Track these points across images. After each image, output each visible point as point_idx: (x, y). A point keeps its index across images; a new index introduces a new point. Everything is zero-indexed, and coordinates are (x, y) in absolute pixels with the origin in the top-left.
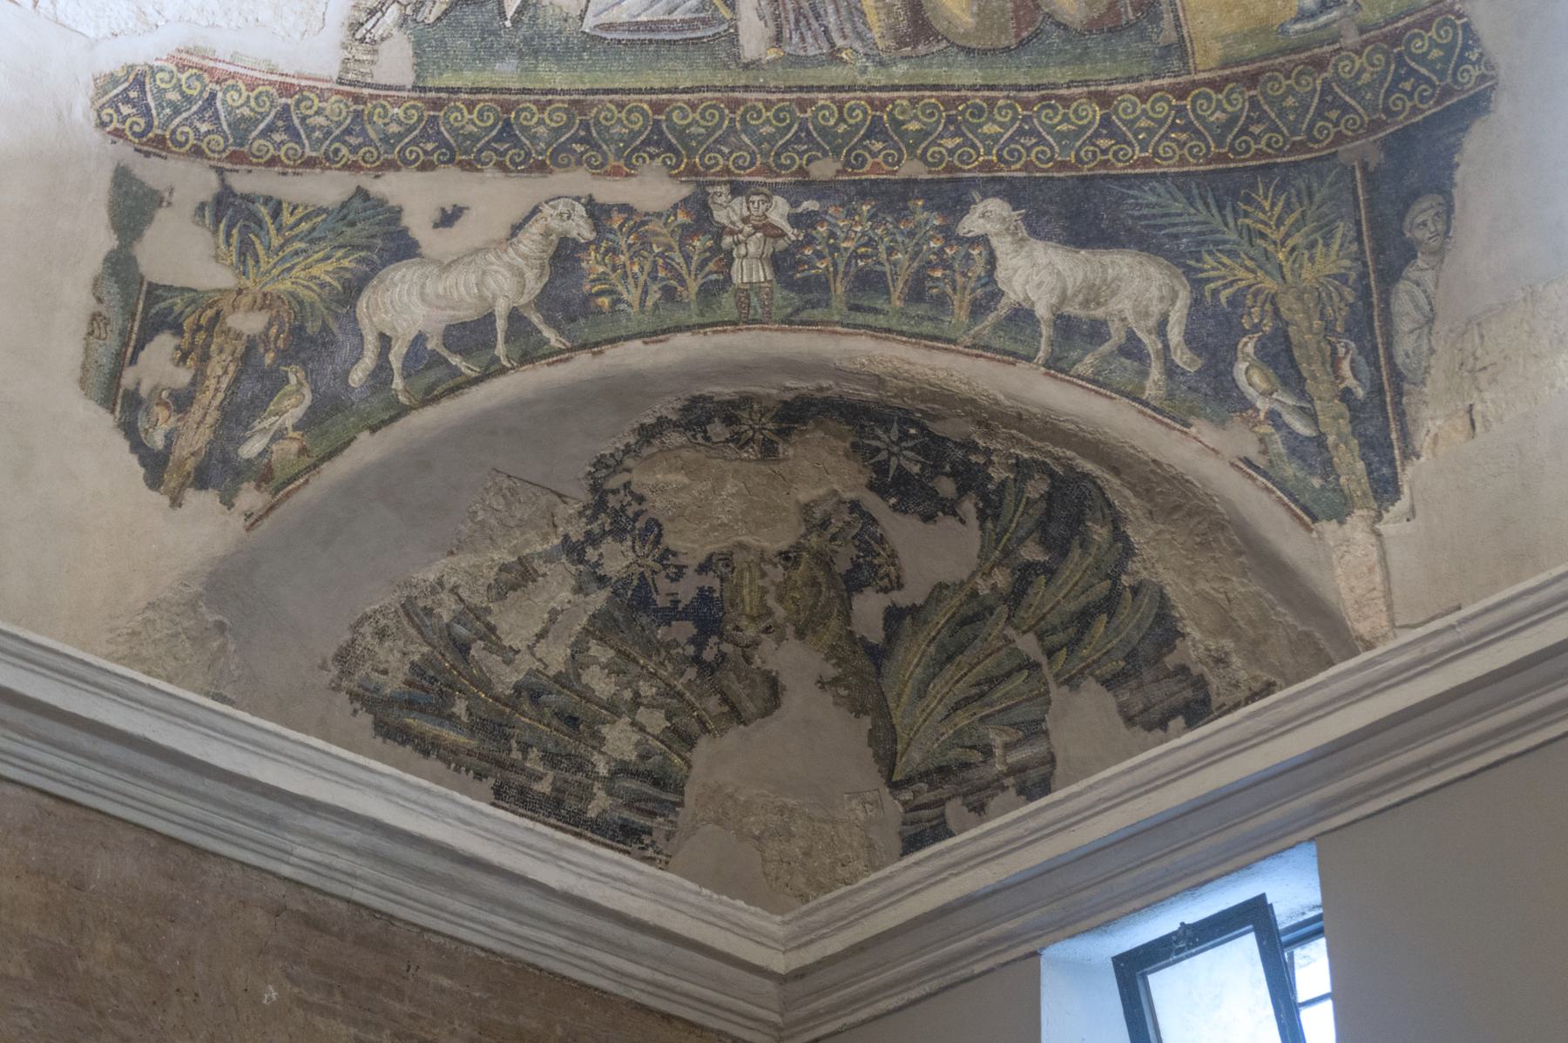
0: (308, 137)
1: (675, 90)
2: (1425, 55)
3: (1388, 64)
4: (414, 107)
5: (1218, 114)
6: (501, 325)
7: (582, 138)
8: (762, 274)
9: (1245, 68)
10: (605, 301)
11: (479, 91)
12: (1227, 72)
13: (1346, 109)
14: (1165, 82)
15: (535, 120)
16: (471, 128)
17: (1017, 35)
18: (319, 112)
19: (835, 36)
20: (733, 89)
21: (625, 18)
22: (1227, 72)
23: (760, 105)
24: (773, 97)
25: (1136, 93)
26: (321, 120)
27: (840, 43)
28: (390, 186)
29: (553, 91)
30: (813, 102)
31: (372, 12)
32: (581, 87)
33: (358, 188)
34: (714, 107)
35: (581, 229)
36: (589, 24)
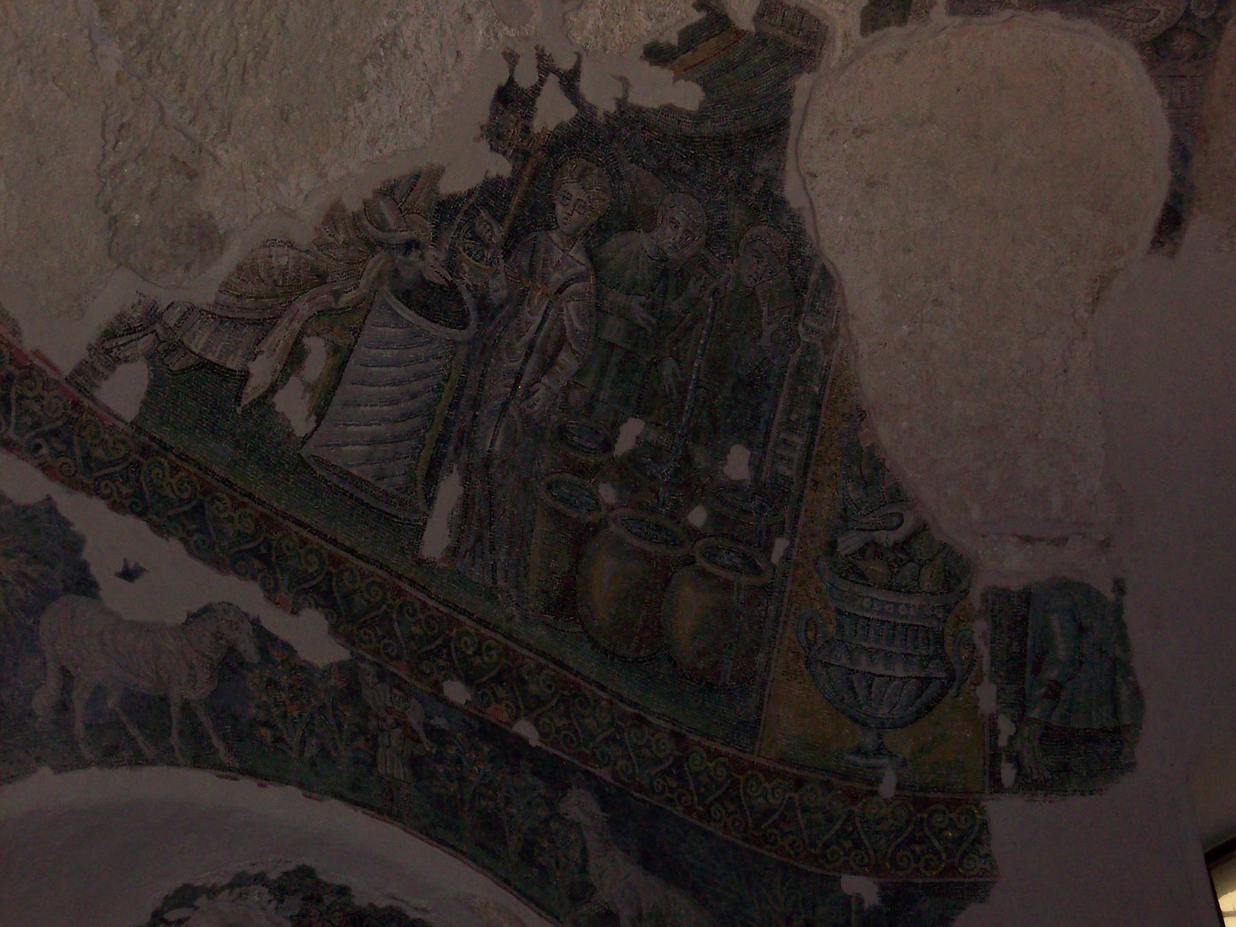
0: (17, 417)
1: (352, 551)
2: (941, 830)
3: (908, 822)
4: (123, 442)
5: (761, 800)
6: (175, 710)
7: (256, 555)
8: (400, 771)
9: (795, 771)
10: (266, 733)
11: (187, 459)
12: (780, 767)
13: (858, 845)
14: (732, 751)
15: (225, 515)
16: (168, 492)
17: (637, 650)
18: (39, 398)
19: (499, 575)
20: (400, 577)
21: (339, 462)
22: (780, 767)
23: (418, 605)
24: (431, 603)
25: (708, 751)
26: (36, 408)
27: (501, 583)
28: (87, 514)
29: (250, 495)
30: (460, 624)
31: (131, 330)
32: (276, 505)
33: (49, 498)
34: (380, 585)
35: (248, 648)
36: (305, 452)
